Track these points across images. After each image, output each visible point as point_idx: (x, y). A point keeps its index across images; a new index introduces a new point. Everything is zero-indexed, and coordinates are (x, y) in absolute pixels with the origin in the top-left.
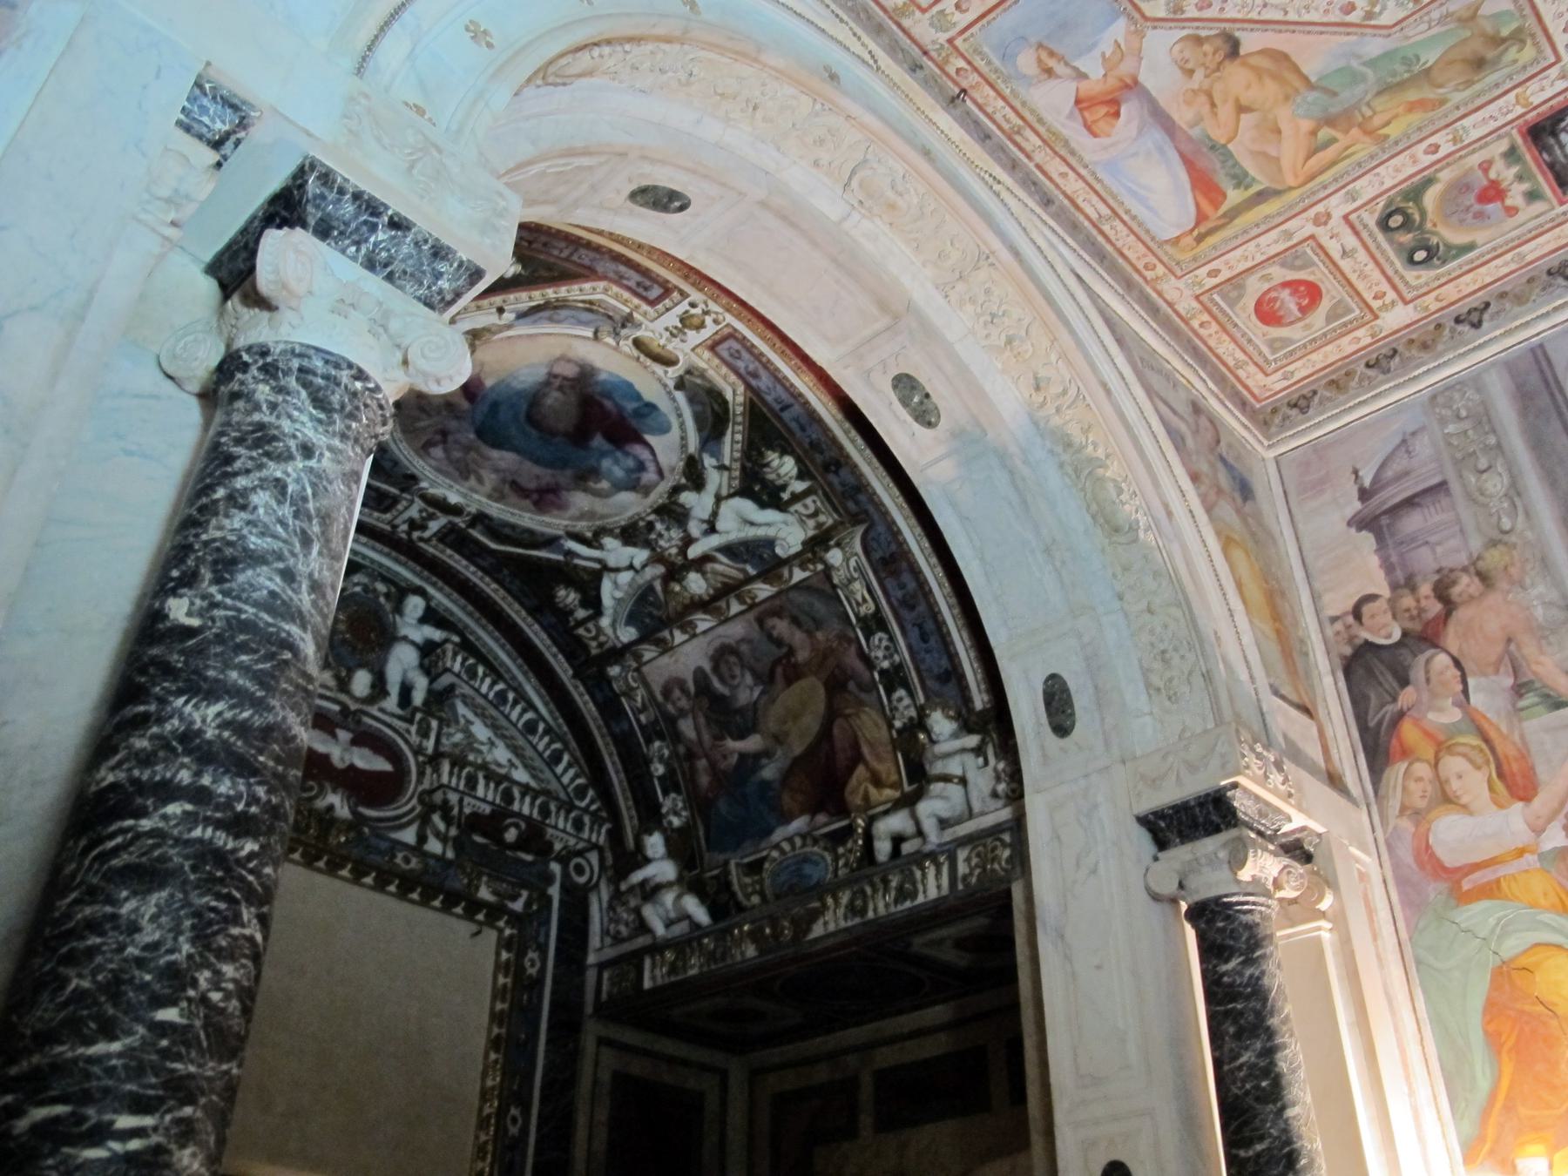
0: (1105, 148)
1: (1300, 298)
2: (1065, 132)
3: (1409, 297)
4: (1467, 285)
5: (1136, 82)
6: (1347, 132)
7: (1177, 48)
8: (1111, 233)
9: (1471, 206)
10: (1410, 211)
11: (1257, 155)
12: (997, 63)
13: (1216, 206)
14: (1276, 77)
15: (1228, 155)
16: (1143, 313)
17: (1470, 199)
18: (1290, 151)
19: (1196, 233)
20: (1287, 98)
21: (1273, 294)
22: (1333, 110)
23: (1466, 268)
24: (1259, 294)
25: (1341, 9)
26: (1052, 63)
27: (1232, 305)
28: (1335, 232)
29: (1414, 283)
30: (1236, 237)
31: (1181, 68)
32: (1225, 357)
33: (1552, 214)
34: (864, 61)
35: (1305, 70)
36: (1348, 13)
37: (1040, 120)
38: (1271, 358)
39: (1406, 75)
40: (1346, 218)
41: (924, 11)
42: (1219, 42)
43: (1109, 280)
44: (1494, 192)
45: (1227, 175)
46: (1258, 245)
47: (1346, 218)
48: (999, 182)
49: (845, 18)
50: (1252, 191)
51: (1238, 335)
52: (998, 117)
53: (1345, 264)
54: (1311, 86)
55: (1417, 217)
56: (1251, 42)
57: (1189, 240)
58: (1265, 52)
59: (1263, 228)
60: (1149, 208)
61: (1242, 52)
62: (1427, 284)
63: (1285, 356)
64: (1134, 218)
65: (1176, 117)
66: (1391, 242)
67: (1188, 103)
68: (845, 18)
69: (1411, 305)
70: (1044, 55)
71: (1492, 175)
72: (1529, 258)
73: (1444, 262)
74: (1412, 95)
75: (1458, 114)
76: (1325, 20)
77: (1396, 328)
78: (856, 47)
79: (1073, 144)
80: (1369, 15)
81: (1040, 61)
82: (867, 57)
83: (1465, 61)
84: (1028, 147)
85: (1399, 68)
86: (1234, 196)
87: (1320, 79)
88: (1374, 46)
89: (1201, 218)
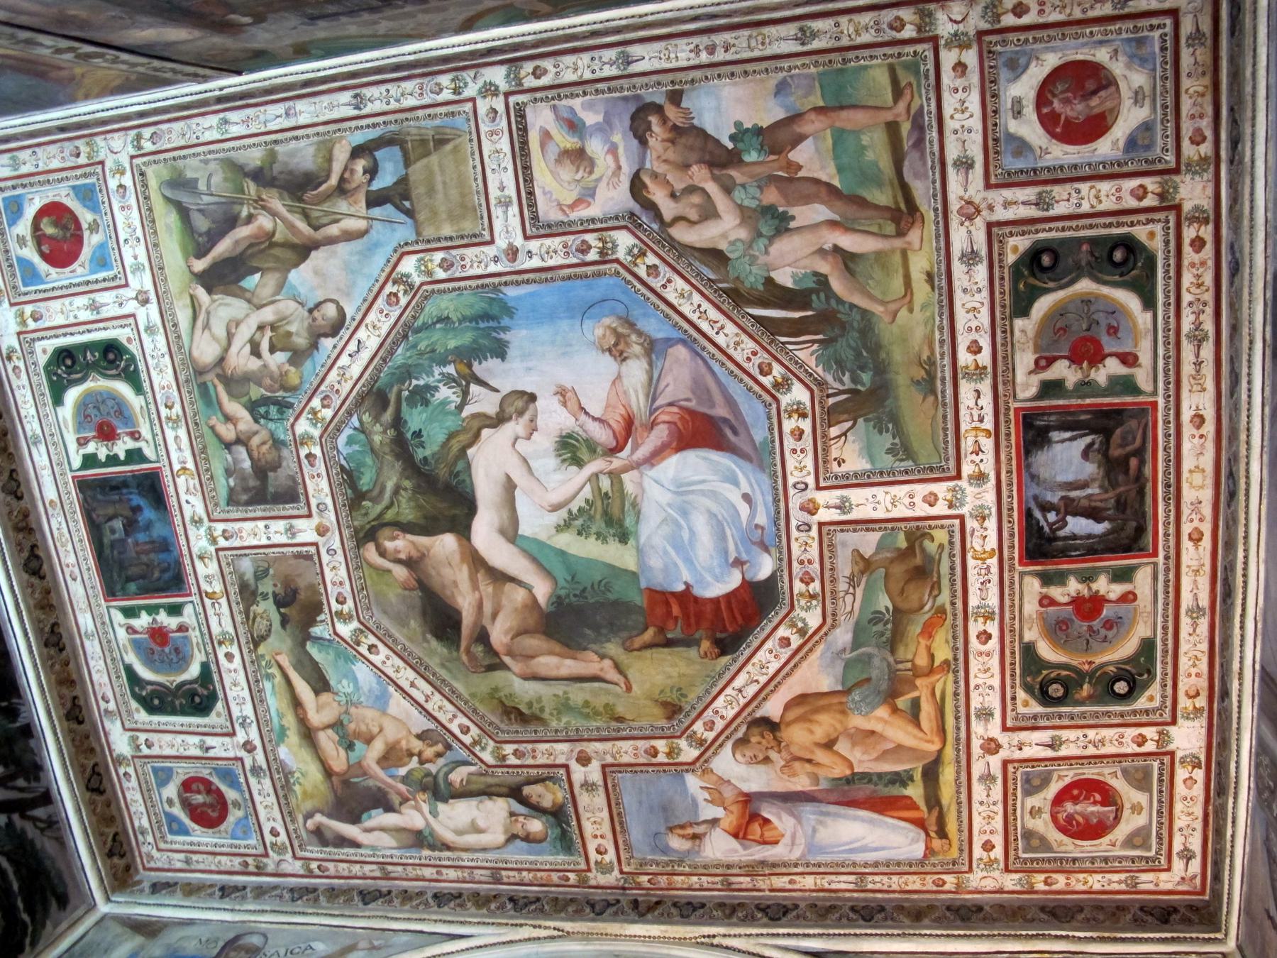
0: (793, 844)
1: (1087, 798)
2: (758, 857)
3: (1167, 717)
4: (1194, 665)
5: (747, 795)
6: (915, 688)
7: (738, 756)
8: (878, 886)
9: (1090, 628)
10: (1052, 675)
11: (884, 755)
12: (666, 858)
13: (914, 806)
14: (817, 710)
15: (866, 777)
16: (939, 932)
17: (1081, 626)
18: (899, 733)
19: (933, 834)
20: (843, 712)
21: (1062, 817)
22: (884, 686)
23: (1169, 659)
24: (1051, 825)
25: (781, 647)
26: (690, 831)
27: (1050, 849)
28: (1015, 743)
29: (1156, 703)
30: (959, 812)
31: (759, 763)
32: (1107, 888)
33: (1161, 567)
34: (552, 938)
35: (825, 689)
36: (789, 644)
37: (729, 867)
38: (1152, 853)
39: (889, 626)
40: (1005, 728)
41: (589, 870)
42: (756, 730)
43: (878, 932)
44: (1089, 606)
45: (886, 785)
46: (981, 803)
47: (1005, 728)
48: (714, 936)
49: (523, 922)
50: (918, 776)
51: (1088, 865)
52: (706, 885)
53: (1063, 752)
54: (847, 692)
55: (1064, 673)
56: (773, 708)
57: (937, 843)
58: (788, 707)
59: (964, 790)
60: (876, 849)
61: (777, 720)
62: (1164, 697)
63: (1160, 843)
64: (876, 864)
65: (799, 788)
66: (1081, 703)
67: (794, 775)
68: (523, 922)
69: (1180, 721)
70: (681, 832)
71: (1065, 599)
72: (1204, 602)
73: (1151, 672)
74: (915, 629)
75: (959, 605)
76: (783, 660)
77: (1203, 743)
78: (543, 933)
79: (771, 860)
80: (802, 632)
81: (683, 836)
82: (556, 933)
83: (907, 582)
84: (750, 886)
85: (880, 627)
86: (915, 791)
87: (843, 684)
88: (842, 636)
89: (920, 823)
